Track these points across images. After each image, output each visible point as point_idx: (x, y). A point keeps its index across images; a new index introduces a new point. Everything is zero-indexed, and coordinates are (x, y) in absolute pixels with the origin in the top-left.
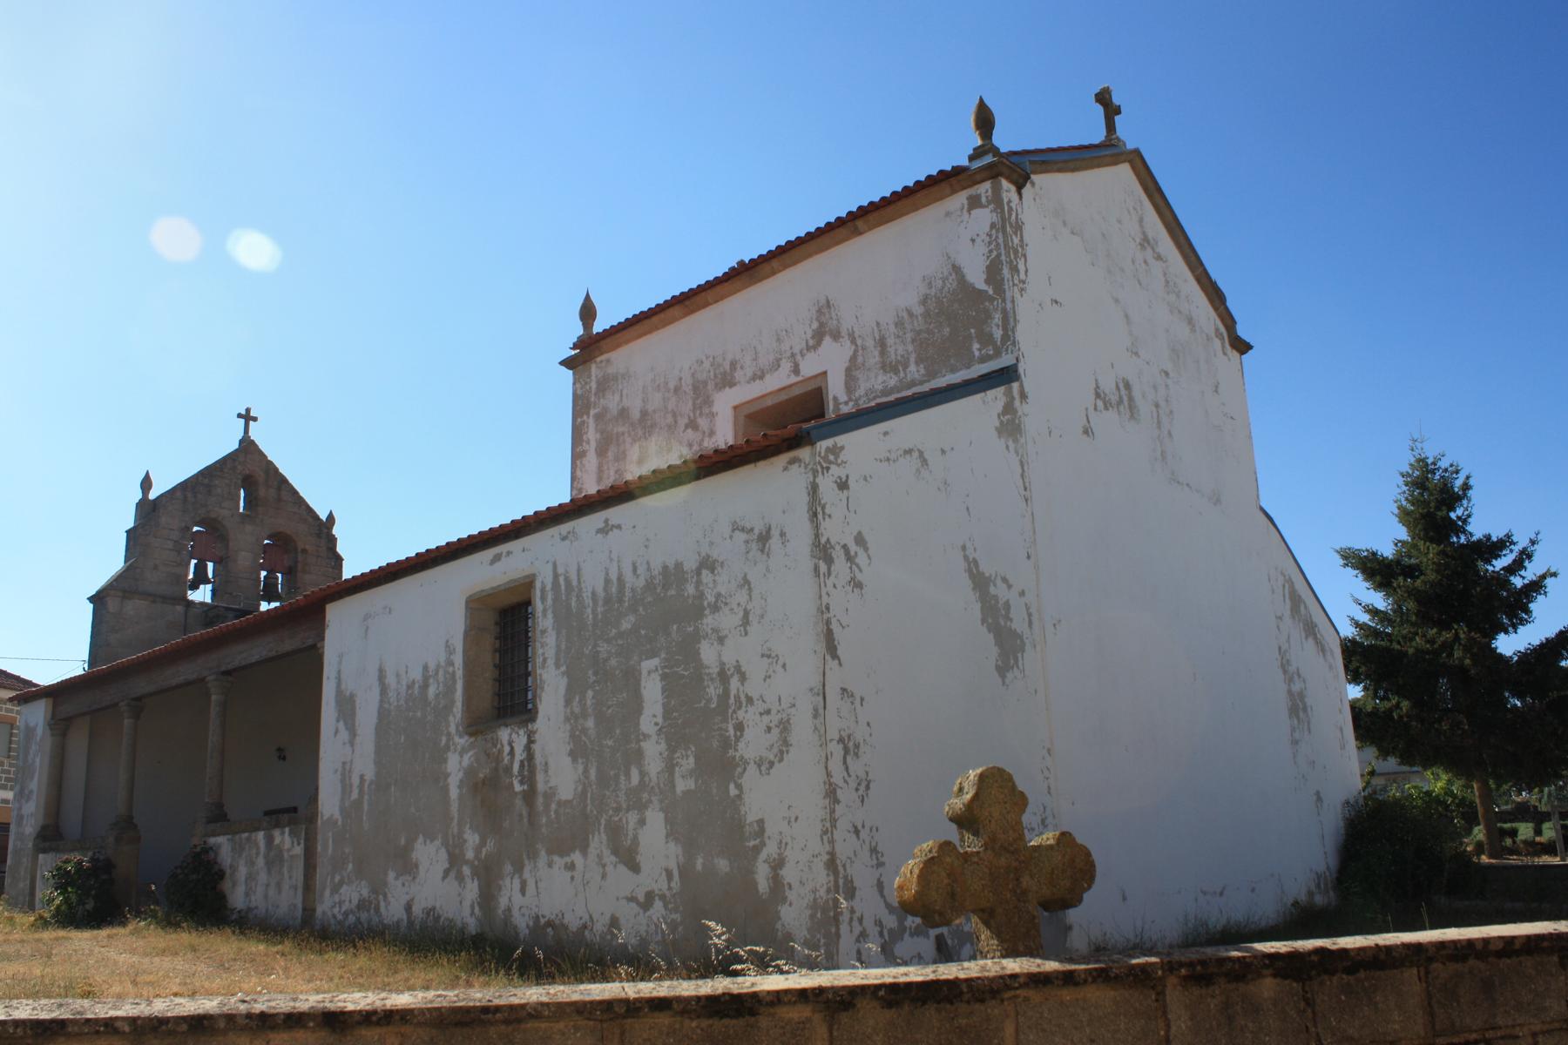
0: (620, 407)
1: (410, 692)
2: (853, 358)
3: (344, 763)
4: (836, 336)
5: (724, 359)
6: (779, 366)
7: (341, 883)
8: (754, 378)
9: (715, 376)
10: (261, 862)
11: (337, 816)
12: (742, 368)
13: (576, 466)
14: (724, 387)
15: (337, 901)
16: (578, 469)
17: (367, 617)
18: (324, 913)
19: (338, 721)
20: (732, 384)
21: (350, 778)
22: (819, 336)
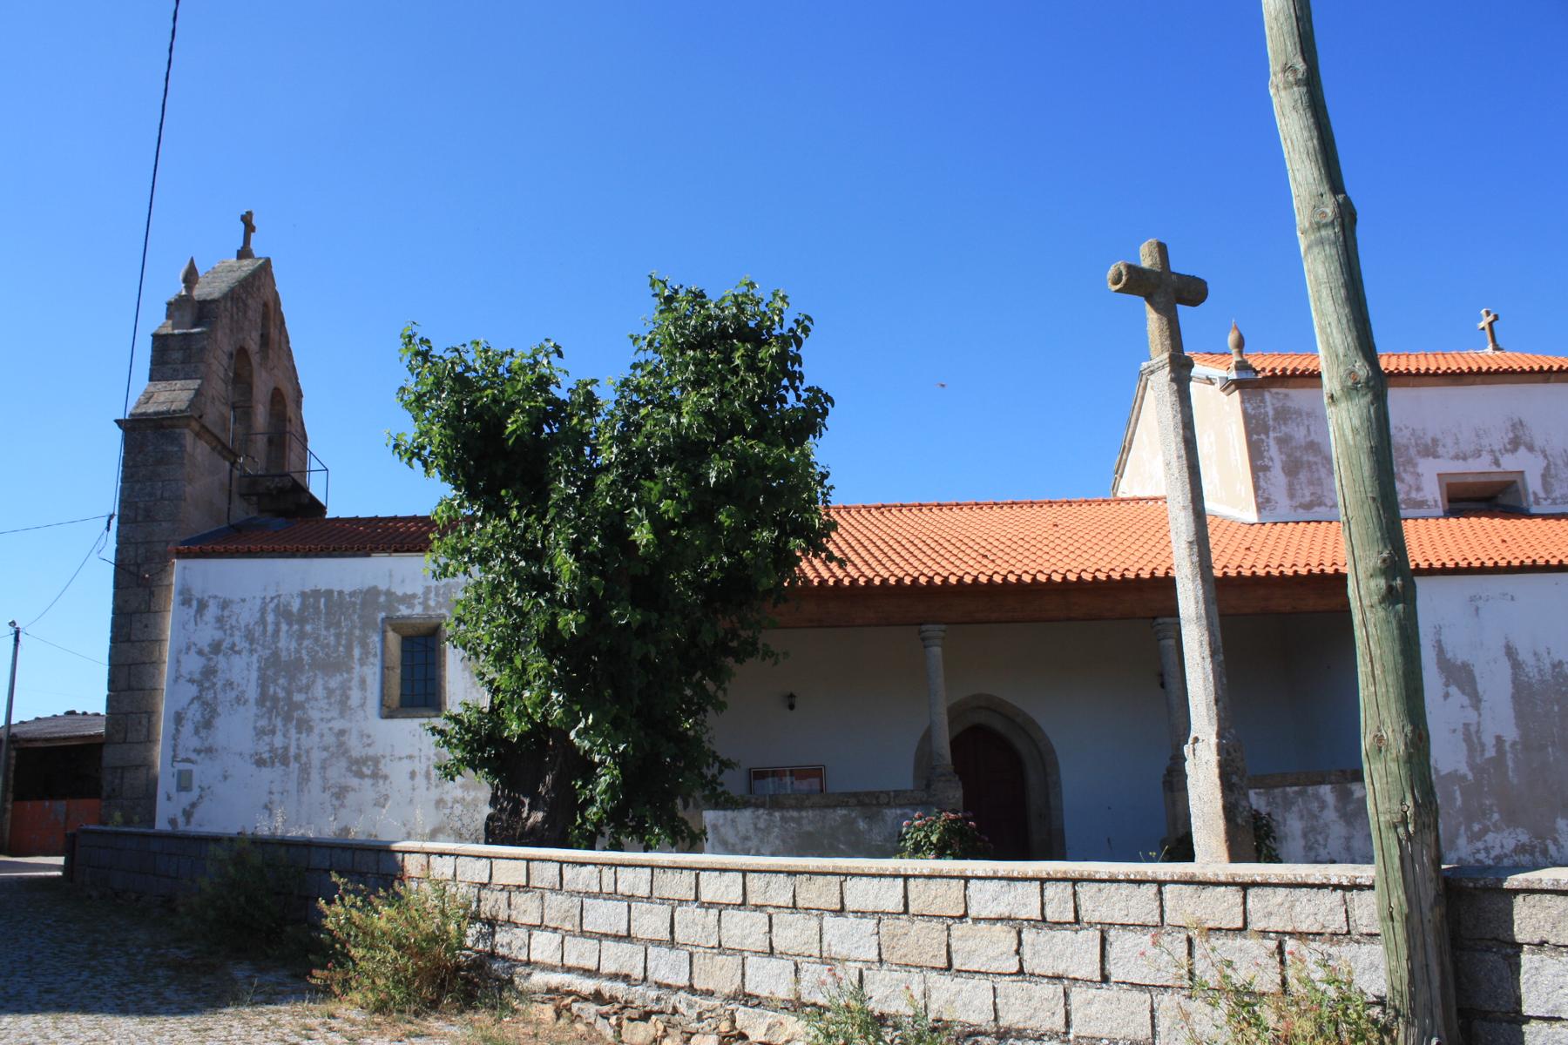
0: (1308, 439)
1: (1557, 670)
2: (1547, 468)
3: (1466, 726)
4: (1531, 448)
5: (1424, 434)
6: (1480, 456)
7: (1485, 831)
8: (1456, 457)
9: (1417, 445)
10: (1330, 815)
11: (1464, 769)
12: (1444, 446)
13: (1258, 477)
14: (1428, 456)
15: (1482, 847)
16: (1261, 480)
17: (1472, 599)
18: (1460, 859)
19: (1447, 685)
20: (1436, 456)
21: (1479, 738)
22: (1515, 444)
